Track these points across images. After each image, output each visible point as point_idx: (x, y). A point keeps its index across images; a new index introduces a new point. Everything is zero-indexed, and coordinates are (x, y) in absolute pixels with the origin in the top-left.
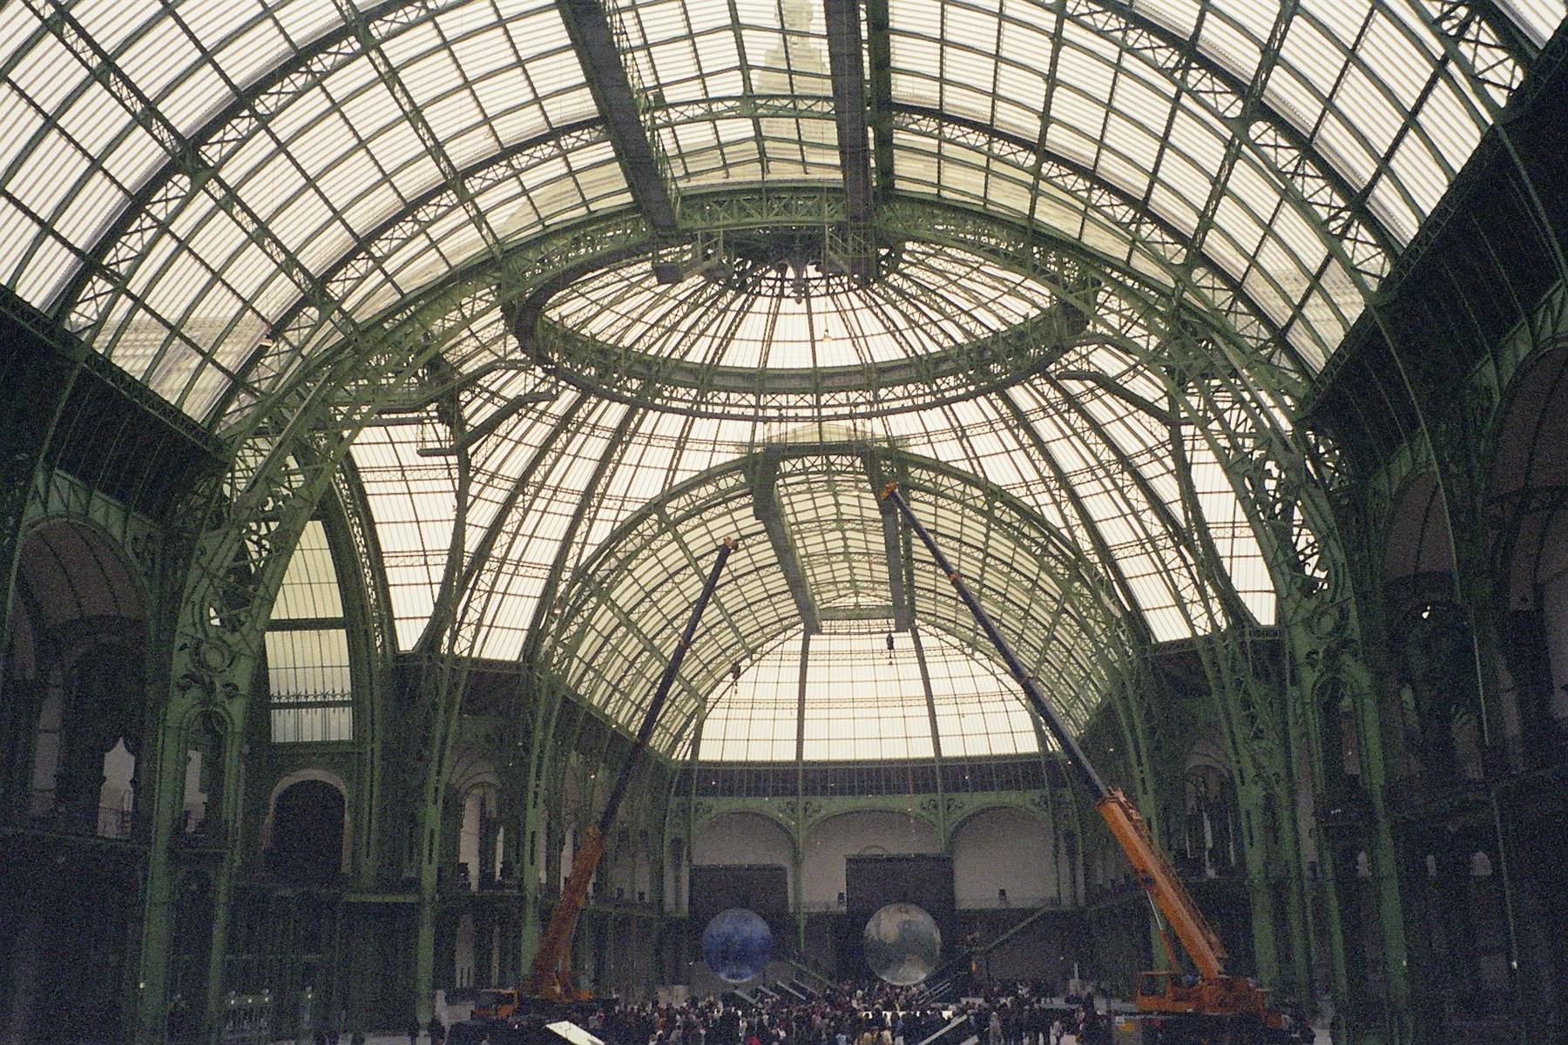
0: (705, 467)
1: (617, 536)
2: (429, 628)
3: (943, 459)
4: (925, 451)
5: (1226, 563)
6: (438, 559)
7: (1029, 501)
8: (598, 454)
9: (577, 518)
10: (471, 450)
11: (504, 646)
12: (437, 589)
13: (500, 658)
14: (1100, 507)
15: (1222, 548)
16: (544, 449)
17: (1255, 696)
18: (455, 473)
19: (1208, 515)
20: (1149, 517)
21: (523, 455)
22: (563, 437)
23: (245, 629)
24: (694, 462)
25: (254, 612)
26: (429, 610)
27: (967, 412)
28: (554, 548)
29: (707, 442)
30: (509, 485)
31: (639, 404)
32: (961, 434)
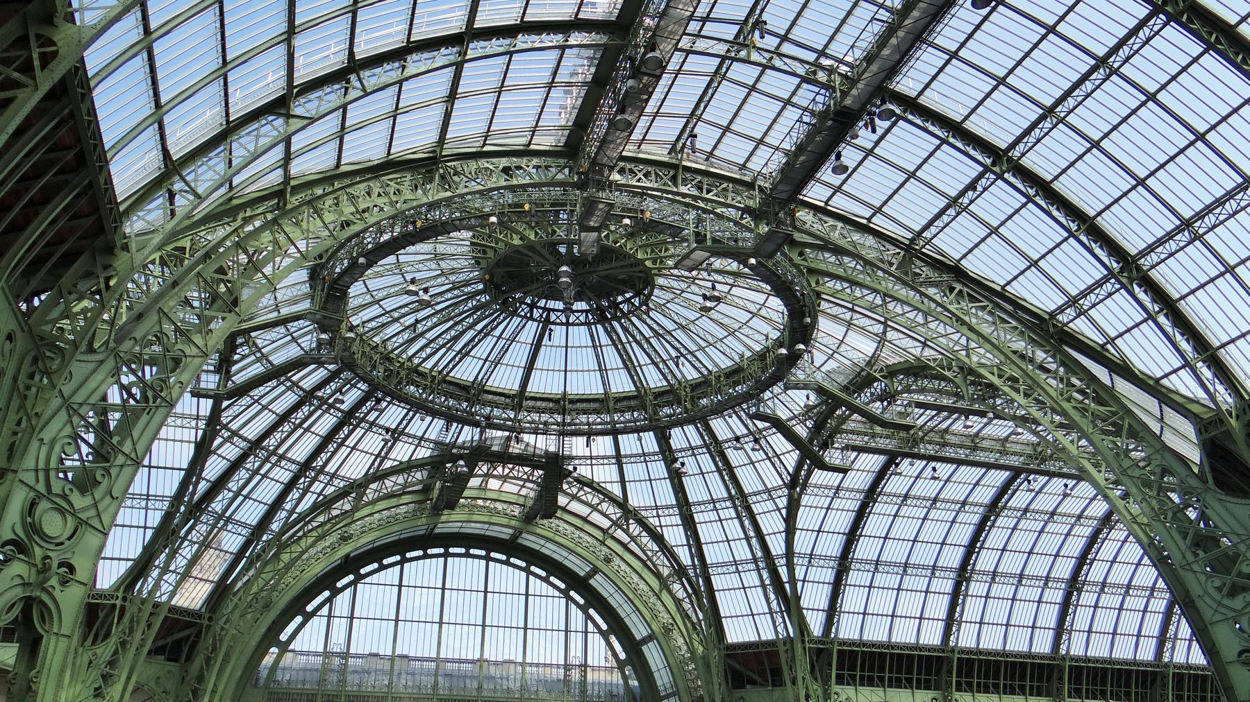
0: (406, 459)
1: (316, 508)
2: (130, 572)
3: (596, 479)
4: (584, 471)
5: (799, 585)
6: (158, 505)
7: (654, 522)
8: (323, 432)
9: (289, 487)
10: (225, 404)
11: (193, 596)
12: (149, 533)
13: (185, 605)
14: (706, 533)
15: (799, 573)
16: (283, 418)
17: (811, 693)
18: (202, 424)
19: (798, 548)
20: (754, 541)
21: (267, 419)
22: (306, 409)
23: (99, 492)
24: (402, 452)
25: (114, 471)
26: (135, 551)
27: (629, 443)
28: (261, 510)
29: (414, 437)
30: (244, 444)
31: (379, 392)
32: (619, 458)
